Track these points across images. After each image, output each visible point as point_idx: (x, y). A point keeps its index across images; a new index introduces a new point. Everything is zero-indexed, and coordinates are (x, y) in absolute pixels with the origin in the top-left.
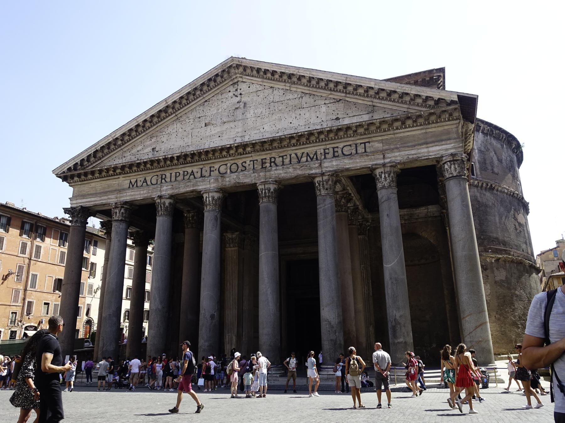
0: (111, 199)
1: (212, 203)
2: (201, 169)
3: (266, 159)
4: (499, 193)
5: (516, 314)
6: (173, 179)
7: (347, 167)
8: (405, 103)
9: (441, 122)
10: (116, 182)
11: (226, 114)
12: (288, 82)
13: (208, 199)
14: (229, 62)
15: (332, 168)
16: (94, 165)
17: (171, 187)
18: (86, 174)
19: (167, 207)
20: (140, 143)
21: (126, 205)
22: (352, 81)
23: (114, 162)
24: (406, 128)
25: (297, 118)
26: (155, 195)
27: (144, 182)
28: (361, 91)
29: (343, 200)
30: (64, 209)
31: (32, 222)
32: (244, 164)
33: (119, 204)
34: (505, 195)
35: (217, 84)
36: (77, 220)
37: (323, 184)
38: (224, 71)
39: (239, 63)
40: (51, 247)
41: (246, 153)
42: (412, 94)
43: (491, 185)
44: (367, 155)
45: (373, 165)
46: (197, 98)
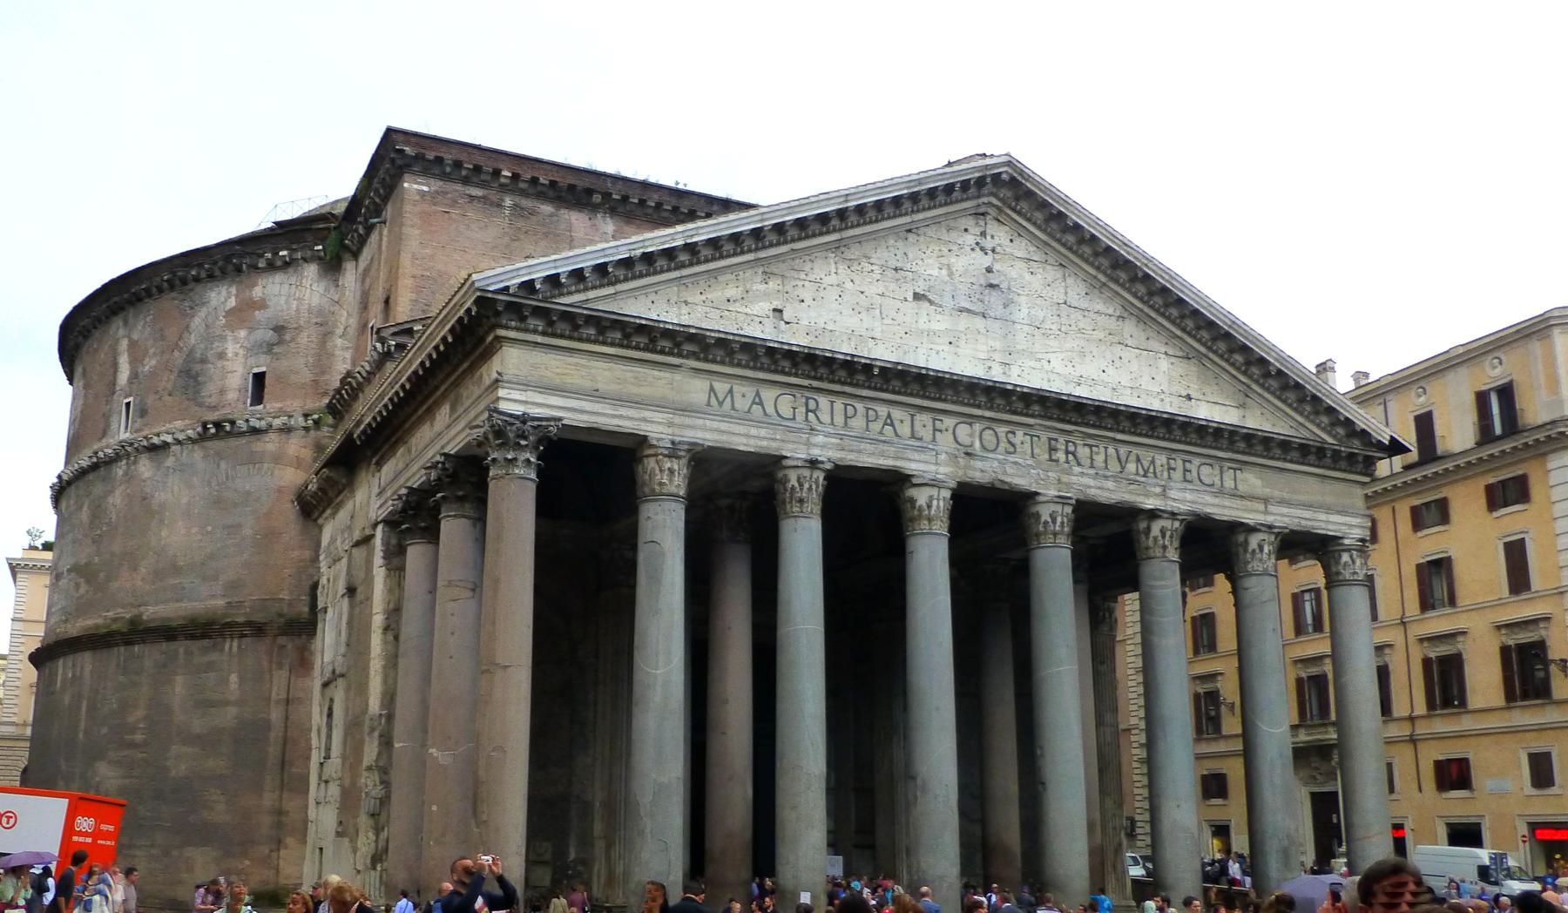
0: (652, 422)
2: (912, 416)
3: (1056, 440)
6: (839, 419)
7: (1208, 510)
10: (662, 374)
11: (963, 288)
12: (1104, 273)
13: (935, 502)
17: (839, 441)
20: (733, 277)
23: (654, 306)
26: (795, 451)
27: (754, 403)
32: (1010, 435)
33: (686, 447)
37: (1171, 537)
41: (1027, 415)
46: (901, 215)
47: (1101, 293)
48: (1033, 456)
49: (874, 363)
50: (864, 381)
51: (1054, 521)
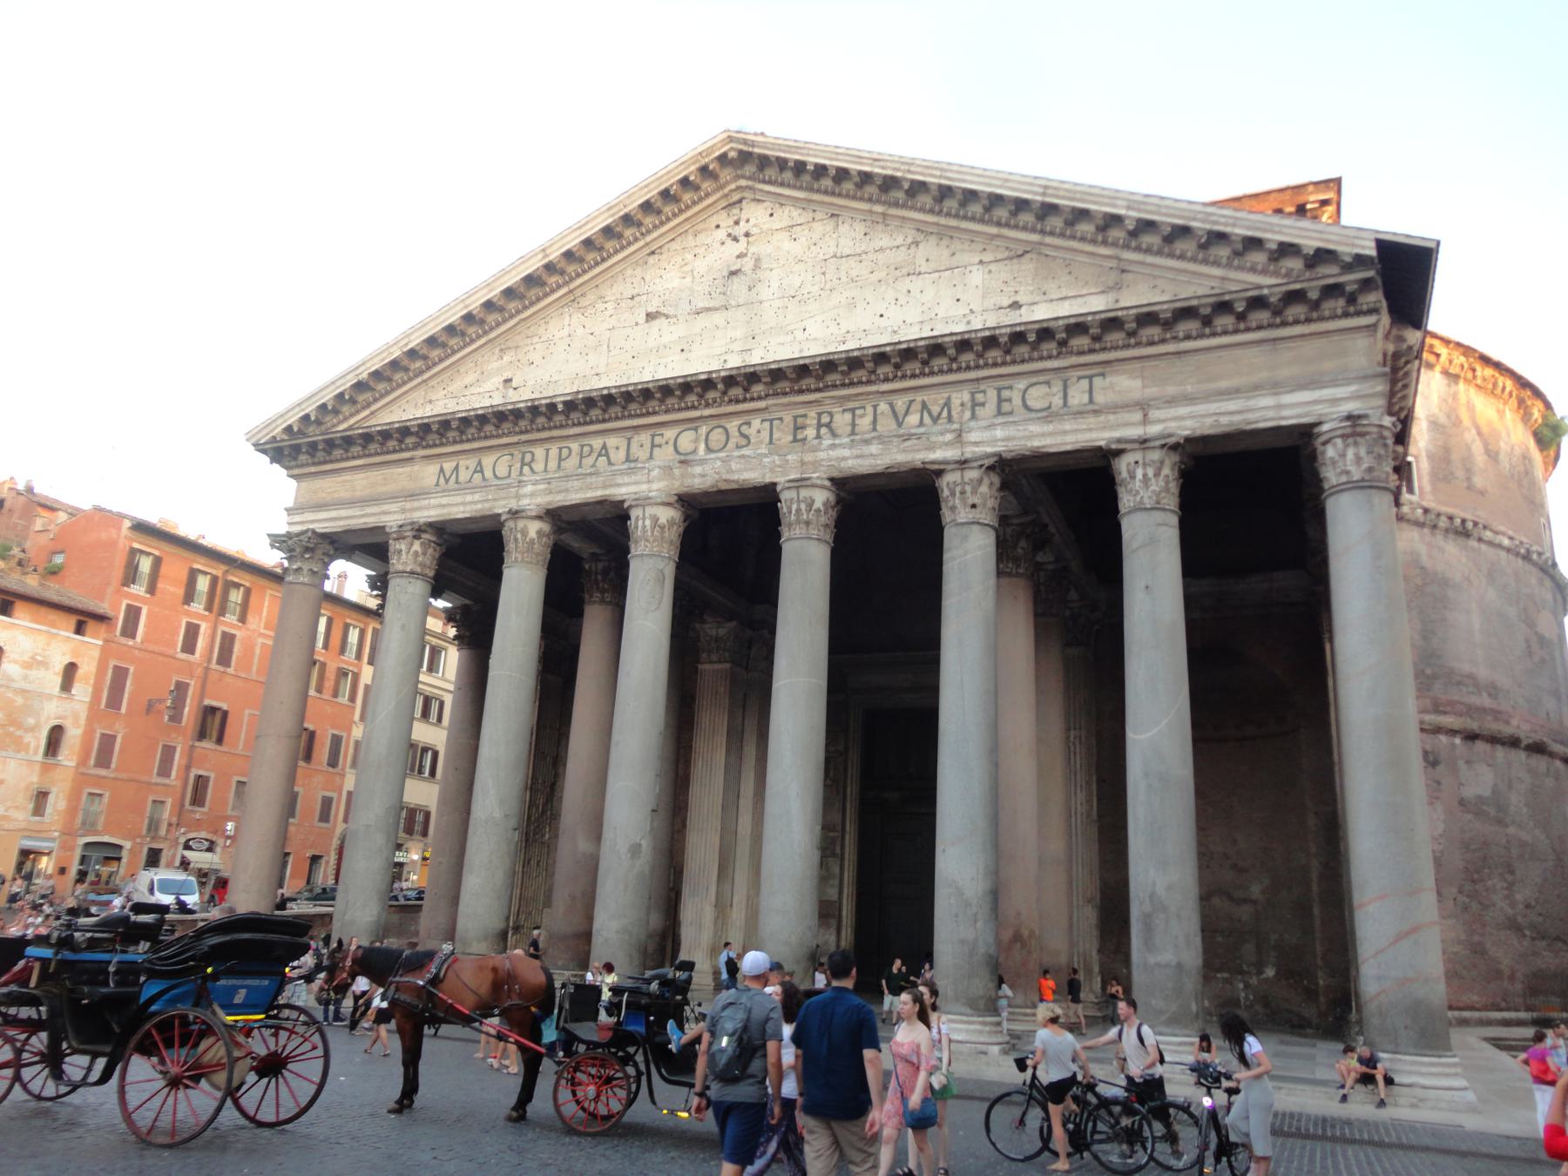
0: (390, 513)
1: (652, 533)
3: (805, 416)
4: (1483, 547)
5: (1519, 897)
6: (553, 464)
7: (1036, 443)
8: (1216, 263)
9: (1322, 319)
12: (879, 202)
13: (640, 523)
14: (719, 145)
15: (996, 446)
16: (352, 421)
17: (547, 486)
18: (330, 444)
19: (532, 542)
20: (471, 365)
21: (425, 531)
22: (1063, 198)
24: (1214, 334)
25: (899, 303)
26: (500, 508)
27: (475, 472)
28: (1086, 228)
29: (1023, 543)
30: (269, 535)
31: (214, 572)
32: (744, 429)
33: (409, 527)
34: (1503, 554)
35: (683, 206)
36: (299, 570)
38: (704, 170)
39: (745, 148)
40: (261, 640)
41: (752, 399)
42: (1237, 235)
43: (1464, 521)
44: (1095, 412)
45: (1111, 441)
46: (629, 244)
47: (887, 225)
48: (771, 442)
49: (554, 401)
50: (566, 420)
51: (791, 512)
